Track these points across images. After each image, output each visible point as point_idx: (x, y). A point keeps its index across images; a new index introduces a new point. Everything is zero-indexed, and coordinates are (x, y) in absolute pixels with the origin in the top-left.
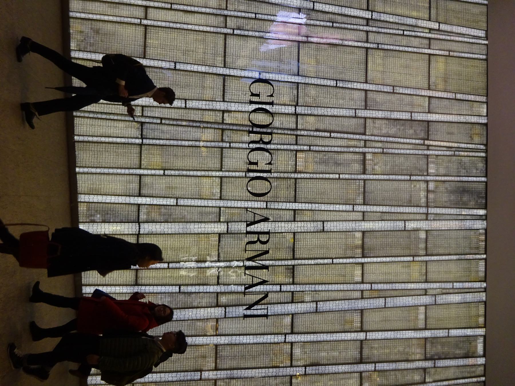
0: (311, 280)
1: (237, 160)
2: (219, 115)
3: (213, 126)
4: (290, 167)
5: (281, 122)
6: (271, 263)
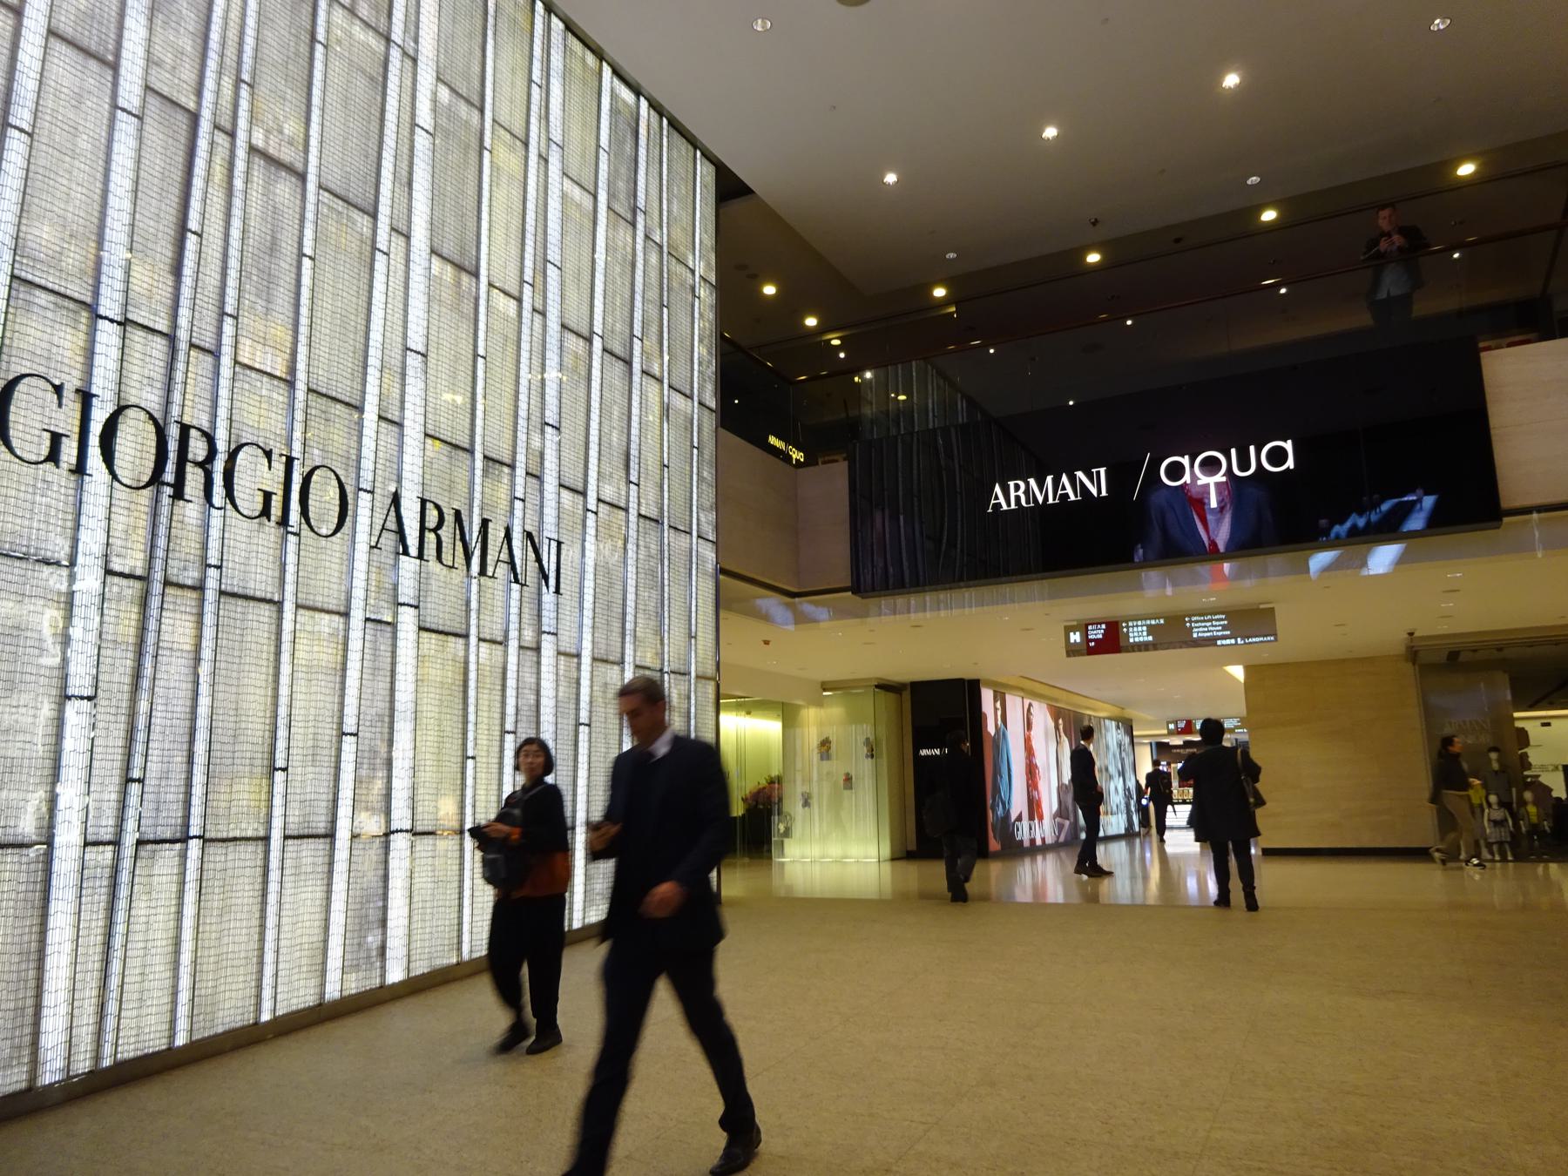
0: (509, 422)
1: (248, 550)
2: (115, 589)
3: (154, 612)
4: (275, 395)
5: (145, 381)
6: (476, 510)
